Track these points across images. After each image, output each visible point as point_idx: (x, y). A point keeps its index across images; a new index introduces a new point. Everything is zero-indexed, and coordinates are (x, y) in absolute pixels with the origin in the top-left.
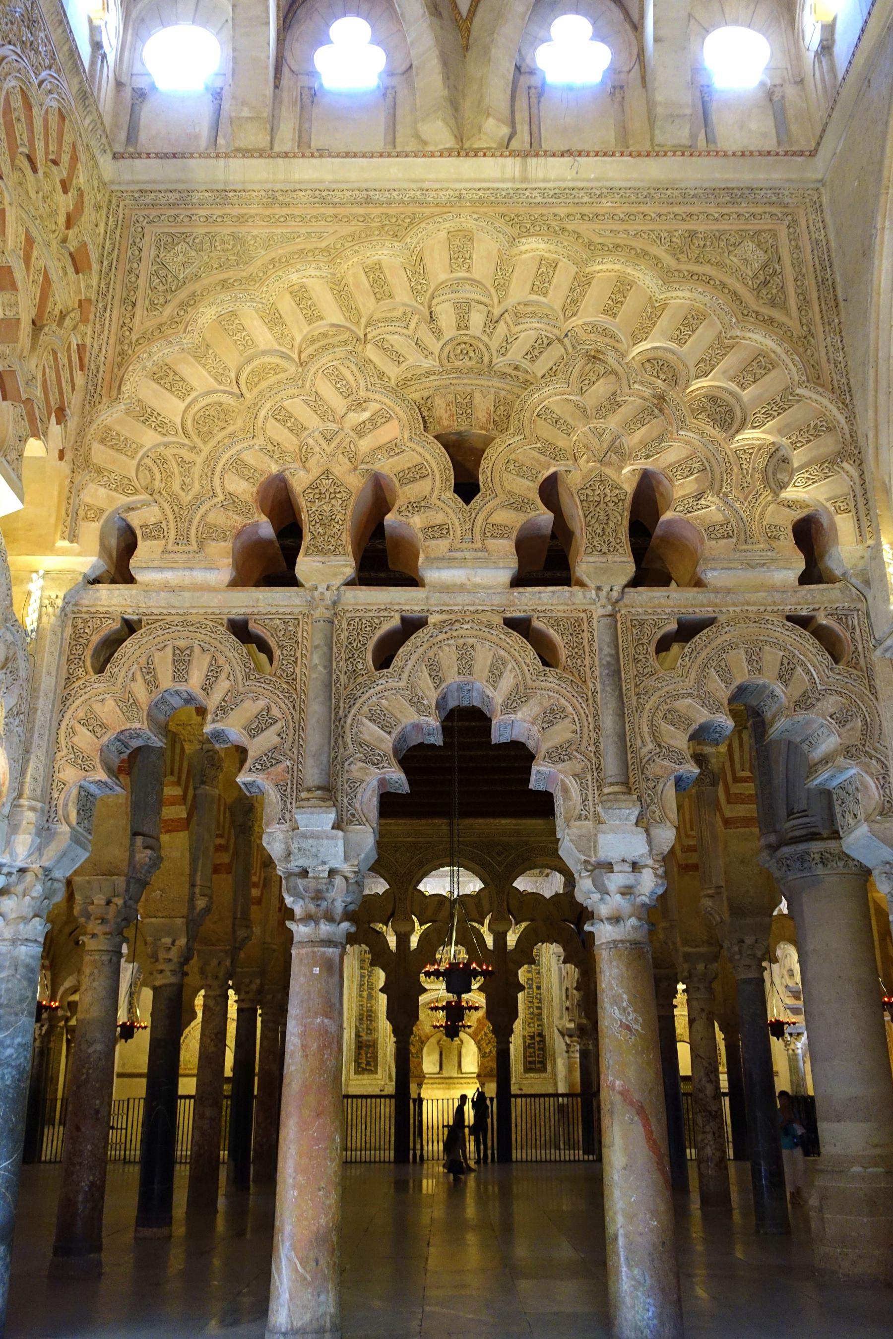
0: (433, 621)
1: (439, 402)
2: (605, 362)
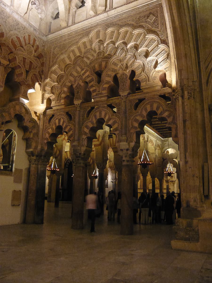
2: (124, 49)
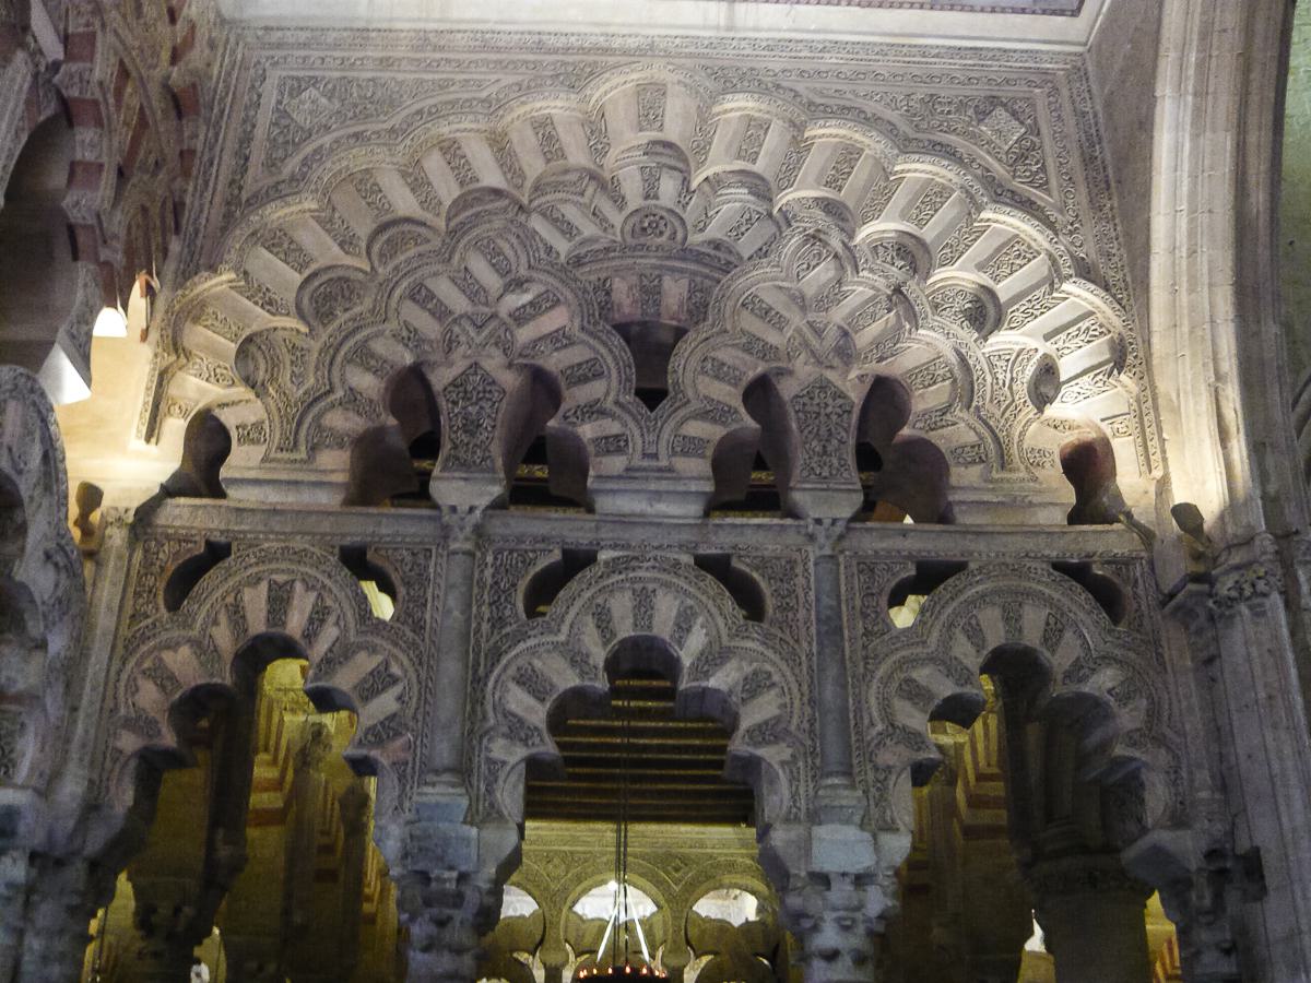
0: (604, 557)
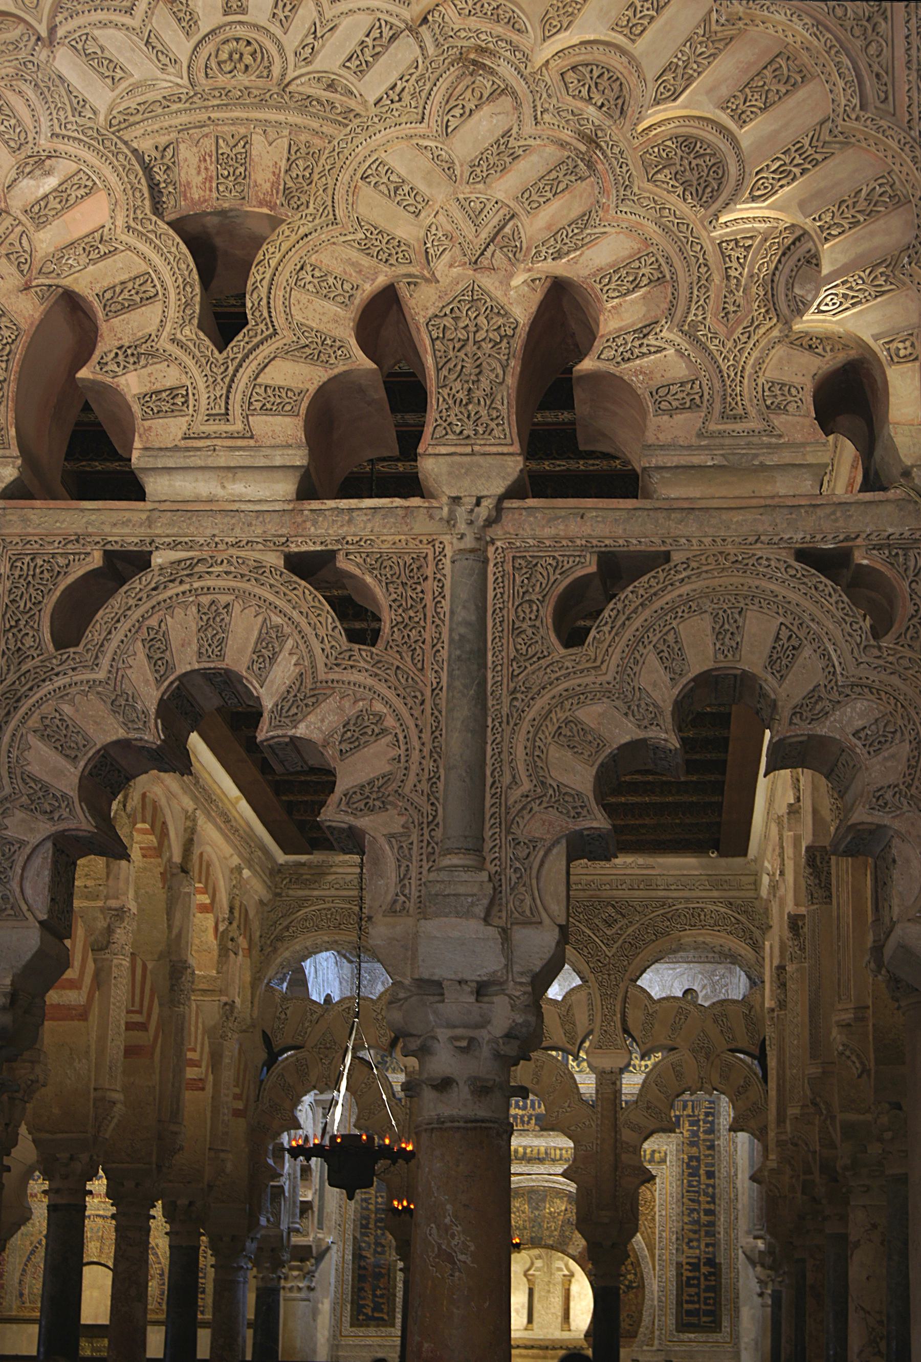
0: (159, 561)
1: (187, 154)
